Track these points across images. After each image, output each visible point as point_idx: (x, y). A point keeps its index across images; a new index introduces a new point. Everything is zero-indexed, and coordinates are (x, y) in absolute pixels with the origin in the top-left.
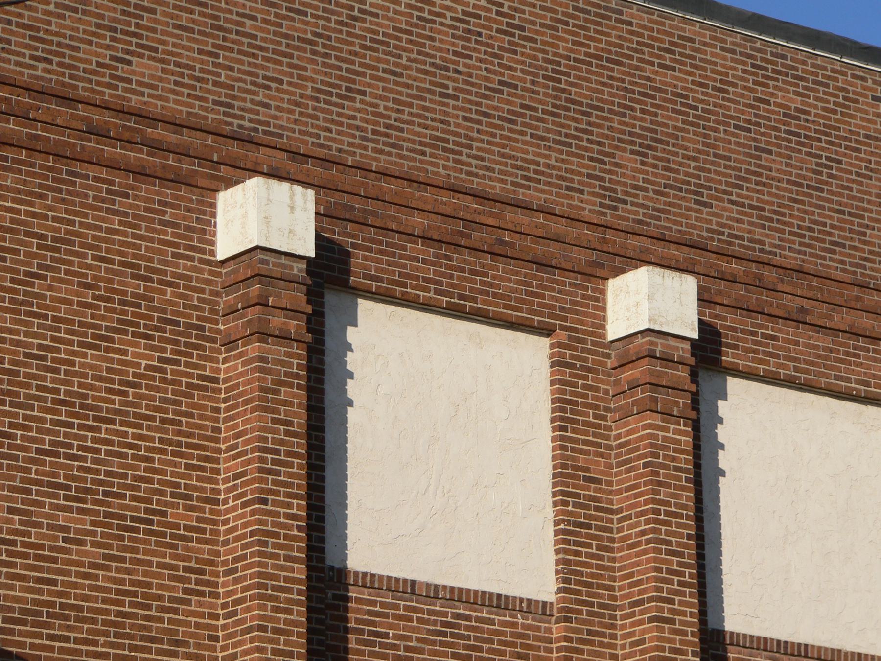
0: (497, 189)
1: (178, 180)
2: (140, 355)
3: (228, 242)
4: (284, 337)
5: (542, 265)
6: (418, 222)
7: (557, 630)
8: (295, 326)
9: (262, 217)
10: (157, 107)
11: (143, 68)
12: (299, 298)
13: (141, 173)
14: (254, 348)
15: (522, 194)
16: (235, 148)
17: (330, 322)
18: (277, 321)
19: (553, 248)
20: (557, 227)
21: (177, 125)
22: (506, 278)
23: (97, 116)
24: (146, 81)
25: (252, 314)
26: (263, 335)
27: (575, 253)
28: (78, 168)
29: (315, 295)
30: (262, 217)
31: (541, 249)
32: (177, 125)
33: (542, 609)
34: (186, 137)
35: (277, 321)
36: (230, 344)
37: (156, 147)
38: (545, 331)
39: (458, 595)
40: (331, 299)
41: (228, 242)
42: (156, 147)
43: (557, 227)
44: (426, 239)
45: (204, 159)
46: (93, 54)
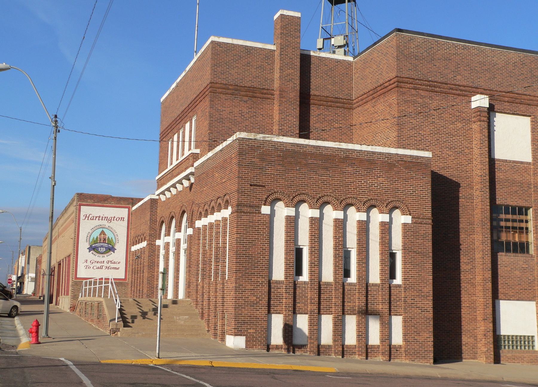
0: (520, 92)
1: (465, 96)
2: (459, 125)
3: (474, 105)
4: (484, 121)
5: (529, 105)
6: (506, 99)
7: (532, 167)
8: (485, 119)
9: (480, 101)
10: (461, 84)
11: (459, 77)
12: (486, 114)
13: (459, 95)
14: (479, 123)
15: (525, 93)
16: (474, 89)
17: (491, 117)
18: (482, 118)
19: (531, 102)
20: (531, 98)
21: (465, 86)
22: (522, 108)
23: (451, 86)
24: (460, 80)
25: (478, 117)
26: (480, 121)
27: (535, 102)
28: (448, 95)
29: (489, 113)
30: (480, 101)
31: (528, 102)
32: (465, 86)
33: (529, 164)
34: (466, 88)
35: (482, 118)
36: (474, 122)
37: (461, 90)
38: (530, 116)
39: (514, 162)
40: (491, 113)
41: (474, 105)
42: (461, 90)
43: (531, 98)
44: (508, 102)
45: (469, 92)
46: (450, 76)
